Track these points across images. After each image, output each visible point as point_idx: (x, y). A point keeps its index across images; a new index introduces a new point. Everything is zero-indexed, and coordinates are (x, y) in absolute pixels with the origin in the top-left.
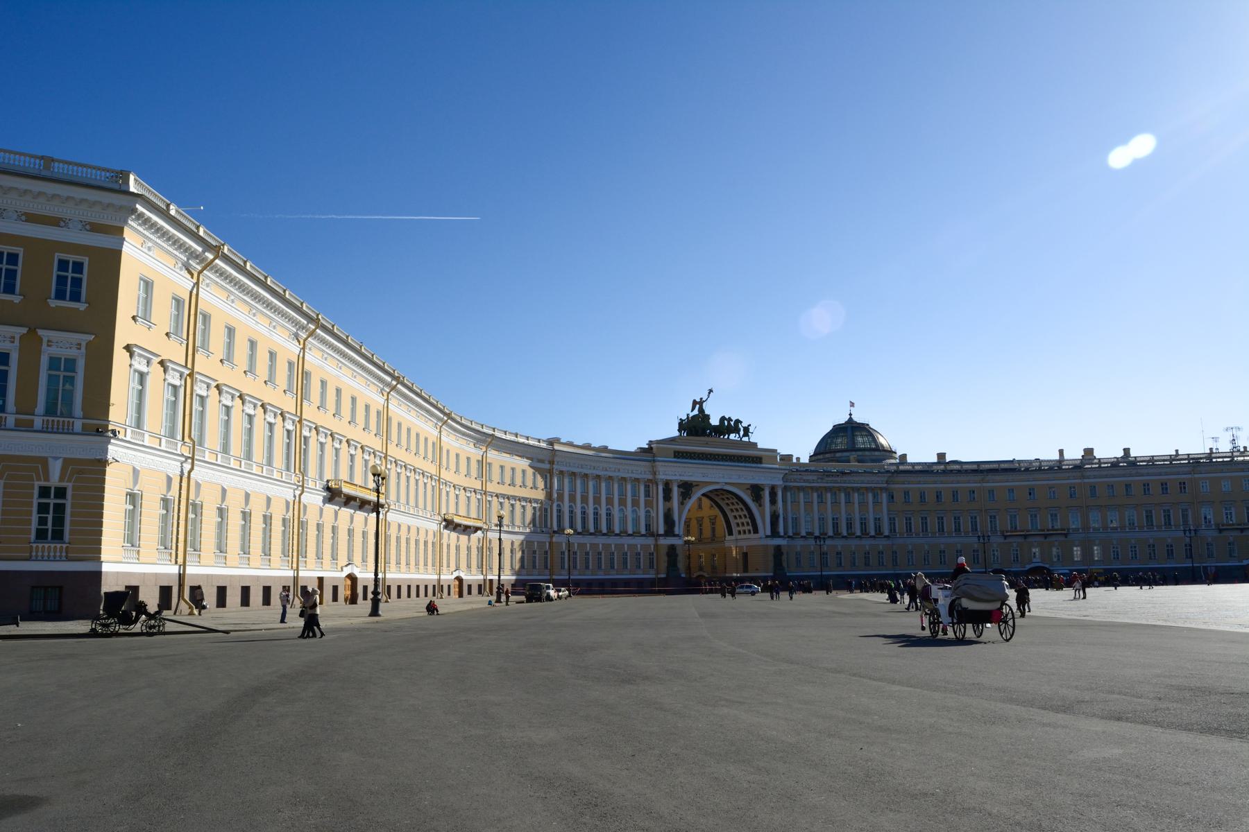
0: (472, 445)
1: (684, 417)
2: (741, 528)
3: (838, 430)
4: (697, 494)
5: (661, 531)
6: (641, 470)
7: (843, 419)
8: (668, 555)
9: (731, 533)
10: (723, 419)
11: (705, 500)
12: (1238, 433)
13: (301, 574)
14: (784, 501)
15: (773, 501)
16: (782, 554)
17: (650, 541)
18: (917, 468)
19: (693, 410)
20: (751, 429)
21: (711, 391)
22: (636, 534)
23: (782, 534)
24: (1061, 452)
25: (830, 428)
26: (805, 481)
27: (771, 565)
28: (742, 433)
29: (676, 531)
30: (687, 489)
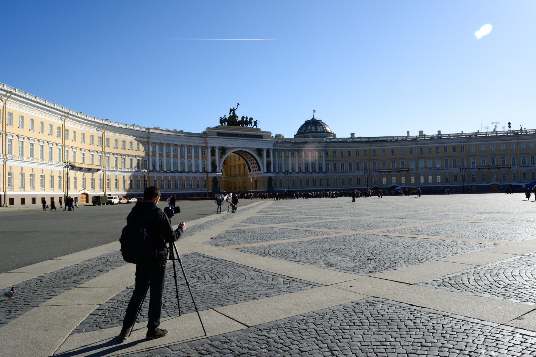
0: (95, 129)
1: (223, 117)
2: (254, 169)
3: (307, 123)
4: (229, 153)
5: (210, 171)
6: (200, 142)
7: (310, 118)
8: (213, 181)
9: (250, 171)
10: (243, 117)
11: (237, 156)
12: (497, 125)
13: (8, 193)
14: (274, 156)
15: (268, 156)
16: (272, 181)
17: (204, 175)
18: (340, 140)
19: (230, 113)
20: (258, 122)
21: (238, 104)
22: (197, 172)
23: (272, 171)
24: (408, 132)
25: (304, 122)
26: (285, 147)
27: (266, 186)
28: (253, 124)
29: (218, 170)
30: (223, 150)
